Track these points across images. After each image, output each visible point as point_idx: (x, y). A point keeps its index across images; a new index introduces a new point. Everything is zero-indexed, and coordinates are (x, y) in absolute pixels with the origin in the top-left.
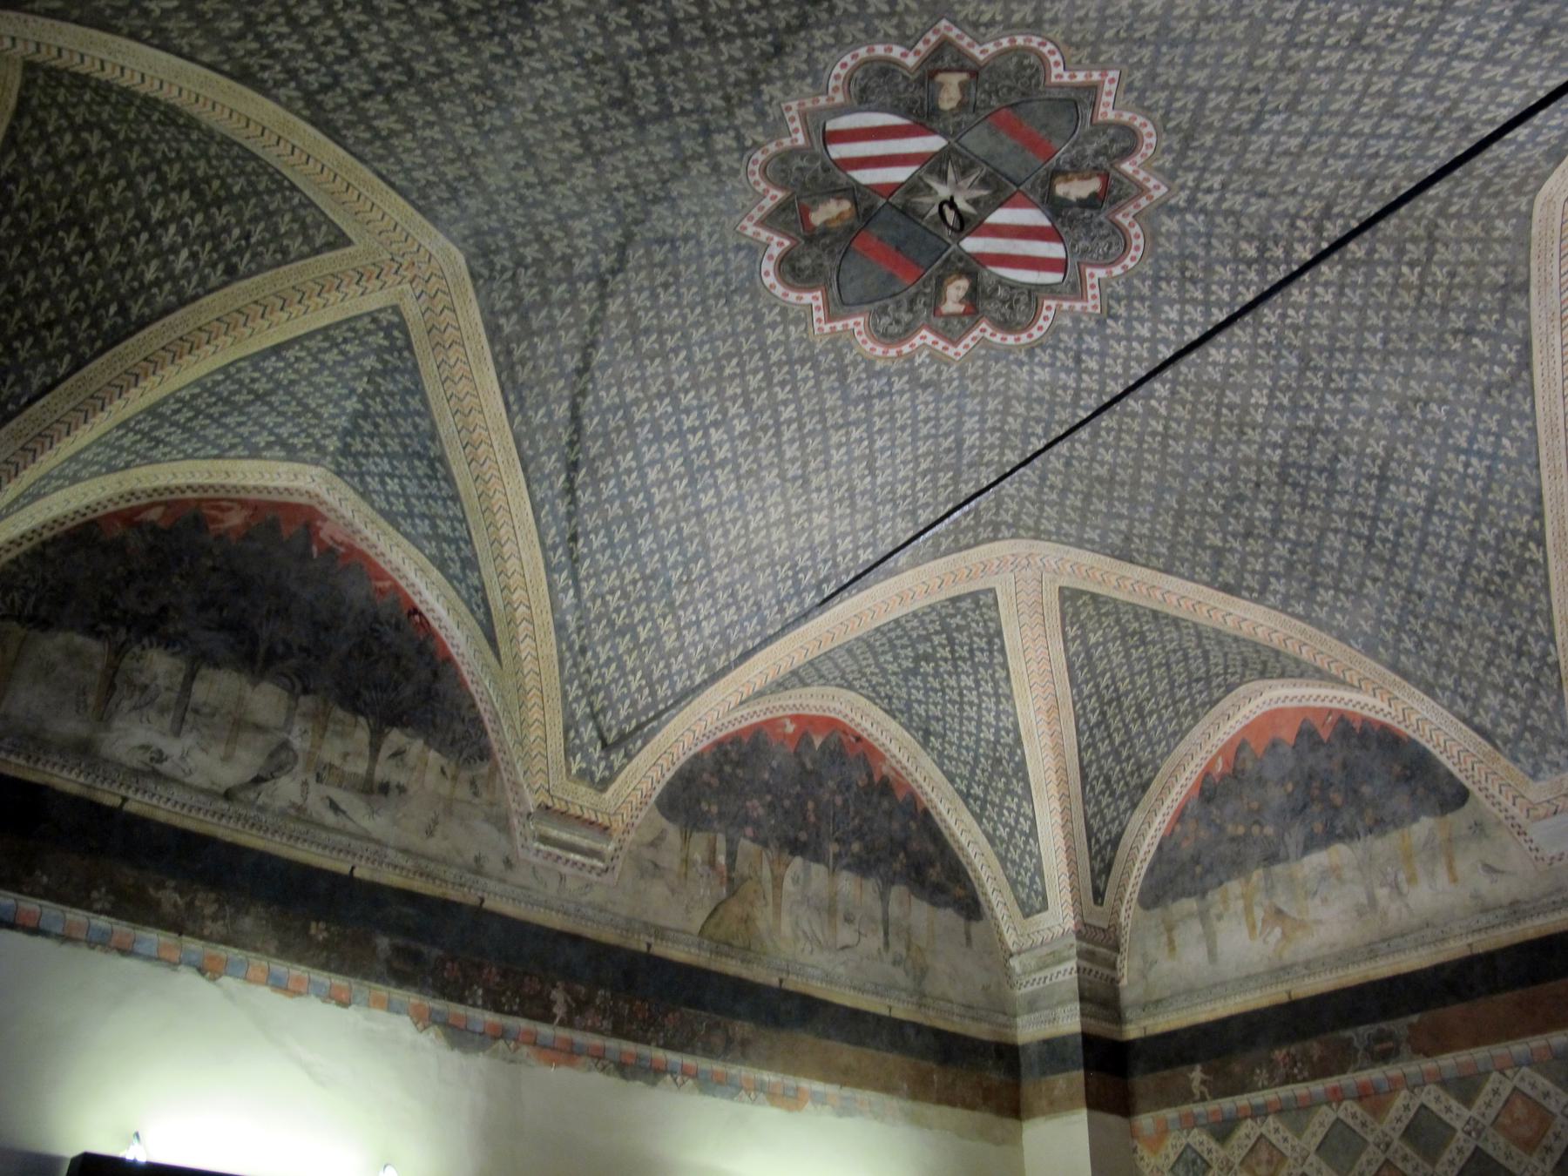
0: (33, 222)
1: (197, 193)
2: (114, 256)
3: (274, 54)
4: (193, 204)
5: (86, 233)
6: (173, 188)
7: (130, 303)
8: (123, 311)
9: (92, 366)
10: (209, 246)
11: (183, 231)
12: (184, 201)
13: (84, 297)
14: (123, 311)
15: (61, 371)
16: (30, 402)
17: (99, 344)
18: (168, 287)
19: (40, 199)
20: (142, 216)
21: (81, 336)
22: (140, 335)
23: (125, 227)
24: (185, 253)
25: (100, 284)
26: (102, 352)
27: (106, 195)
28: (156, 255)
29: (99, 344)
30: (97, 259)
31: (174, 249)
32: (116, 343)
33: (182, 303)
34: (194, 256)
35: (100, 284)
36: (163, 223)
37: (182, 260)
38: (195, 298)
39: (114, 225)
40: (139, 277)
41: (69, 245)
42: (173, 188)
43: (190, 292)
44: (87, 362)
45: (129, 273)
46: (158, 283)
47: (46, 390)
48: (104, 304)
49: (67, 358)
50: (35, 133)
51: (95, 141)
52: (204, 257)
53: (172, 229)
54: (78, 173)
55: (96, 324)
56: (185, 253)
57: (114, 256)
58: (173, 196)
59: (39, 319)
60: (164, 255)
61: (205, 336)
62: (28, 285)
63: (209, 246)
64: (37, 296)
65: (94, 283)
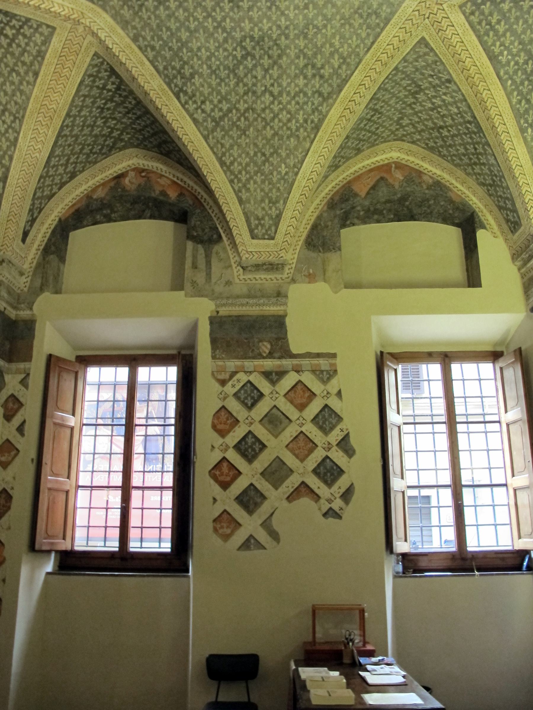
0: (440, 143)
1: (417, 93)
2: (449, 121)
3: (306, 121)
4: (422, 94)
5: (441, 127)
6: (417, 100)
7: (466, 119)
8: (470, 122)
9: (489, 141)
10: (439, 89)
11: (435, 97)
12: (421, 97)
13: (465, 134)
14: (470, 122)
15: (491, 152)
16: (499, 166)
17: (481, 135)
18: (459, 105)
19: (432, 138)
20: (432, 110)
21: (479, 140)
22: (479, 119)
23: (437, 115)
24: (444, 97)
25: (460, 127)
26: (484, 135)
27: (426, 120)
28: (447, 107)
29: (481, 135)
30: (451, 126)
31: (444, 101)
32: (481, 128)
33: (466, 100)
34: (445, 94)
35: (460, 127)
36: (433, 104)
37: (448, 99)
38: (463, 95)
39: (437, 118)
40: (456, 114)
41: (447, 134)
42: (417, 100)
43: (461, 97)
44: (488, 141)
45: (455, 117)
46: (458, 108)
47: (495, 159)
48: (467, 128)
49: (486, 147)
50: (408, 137)
51: (405, 121)
52: (444, 91)
53: (434, 100)
54: (420, 127)
55: (475, 133)
56: (444, 97)
57: (449, 121)
58: (420, 100)
59: (473, 151)
60: (446, 104)
61: (479, 95)
62: (462, 150)
63: (439, 89)
64: (466, 149)
65: (460, 130)
